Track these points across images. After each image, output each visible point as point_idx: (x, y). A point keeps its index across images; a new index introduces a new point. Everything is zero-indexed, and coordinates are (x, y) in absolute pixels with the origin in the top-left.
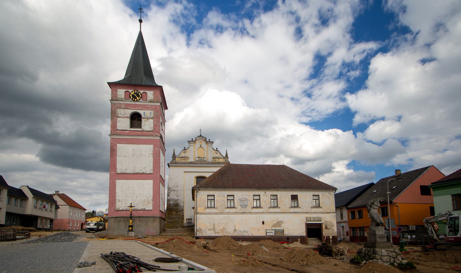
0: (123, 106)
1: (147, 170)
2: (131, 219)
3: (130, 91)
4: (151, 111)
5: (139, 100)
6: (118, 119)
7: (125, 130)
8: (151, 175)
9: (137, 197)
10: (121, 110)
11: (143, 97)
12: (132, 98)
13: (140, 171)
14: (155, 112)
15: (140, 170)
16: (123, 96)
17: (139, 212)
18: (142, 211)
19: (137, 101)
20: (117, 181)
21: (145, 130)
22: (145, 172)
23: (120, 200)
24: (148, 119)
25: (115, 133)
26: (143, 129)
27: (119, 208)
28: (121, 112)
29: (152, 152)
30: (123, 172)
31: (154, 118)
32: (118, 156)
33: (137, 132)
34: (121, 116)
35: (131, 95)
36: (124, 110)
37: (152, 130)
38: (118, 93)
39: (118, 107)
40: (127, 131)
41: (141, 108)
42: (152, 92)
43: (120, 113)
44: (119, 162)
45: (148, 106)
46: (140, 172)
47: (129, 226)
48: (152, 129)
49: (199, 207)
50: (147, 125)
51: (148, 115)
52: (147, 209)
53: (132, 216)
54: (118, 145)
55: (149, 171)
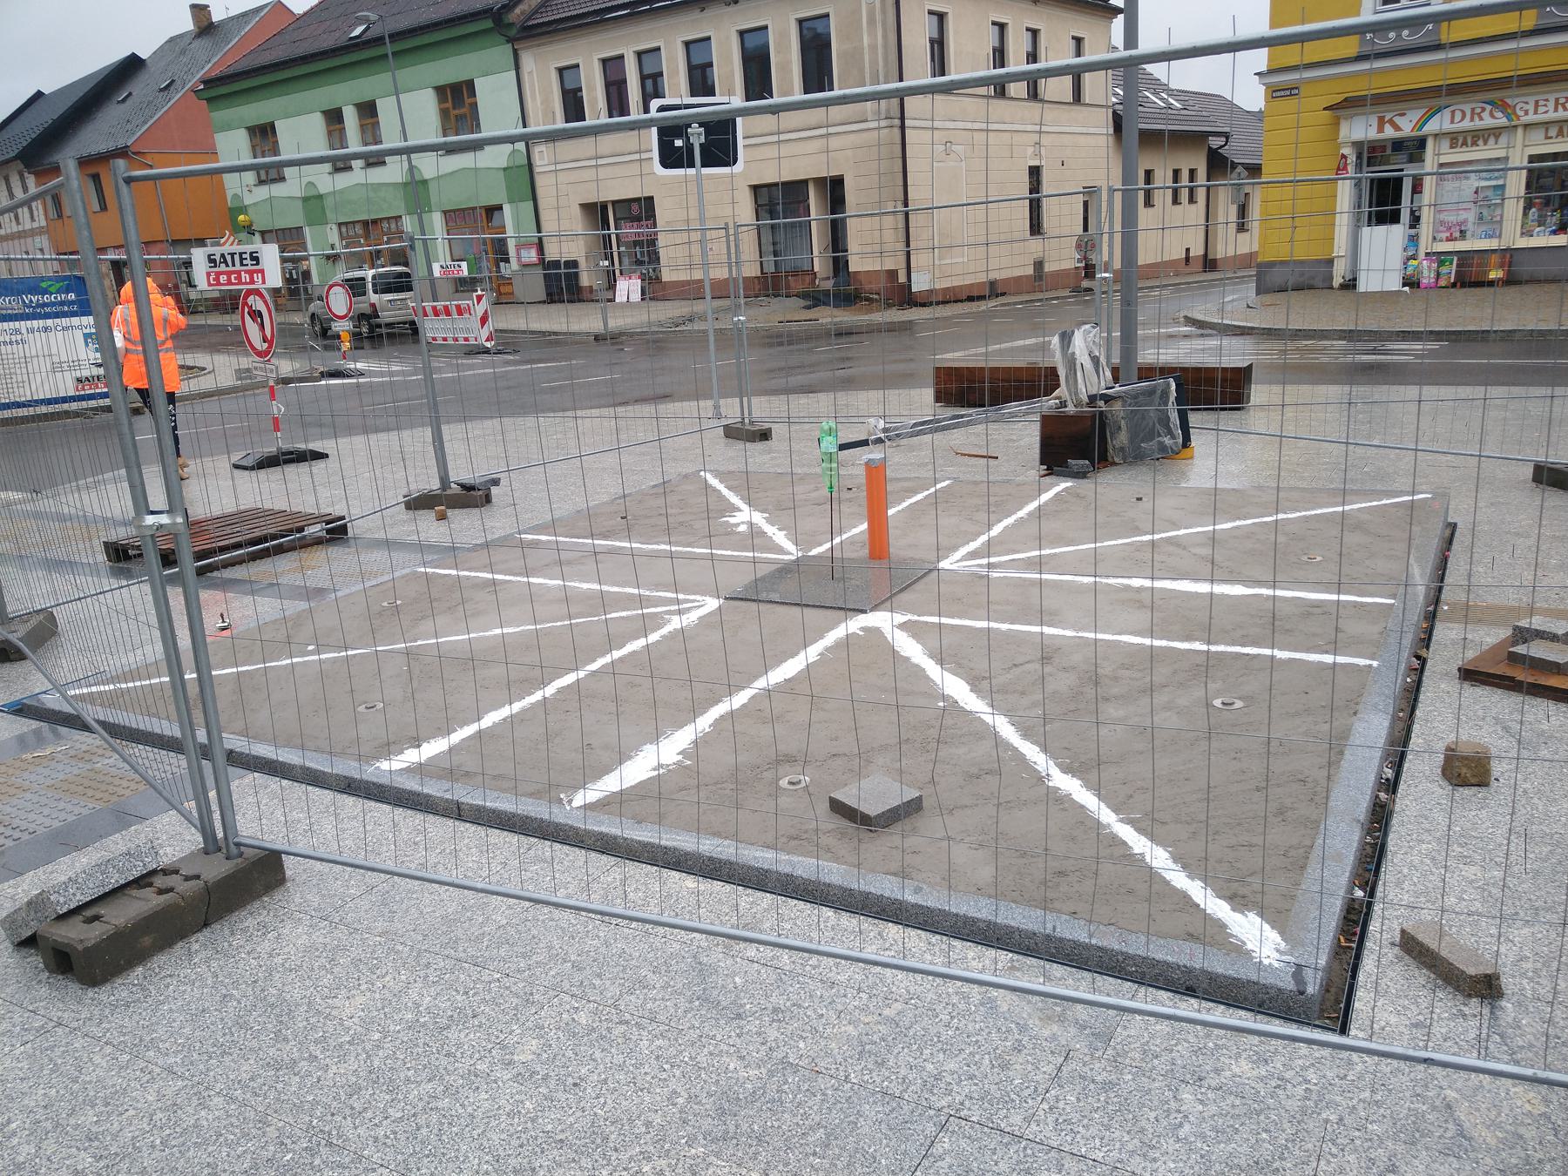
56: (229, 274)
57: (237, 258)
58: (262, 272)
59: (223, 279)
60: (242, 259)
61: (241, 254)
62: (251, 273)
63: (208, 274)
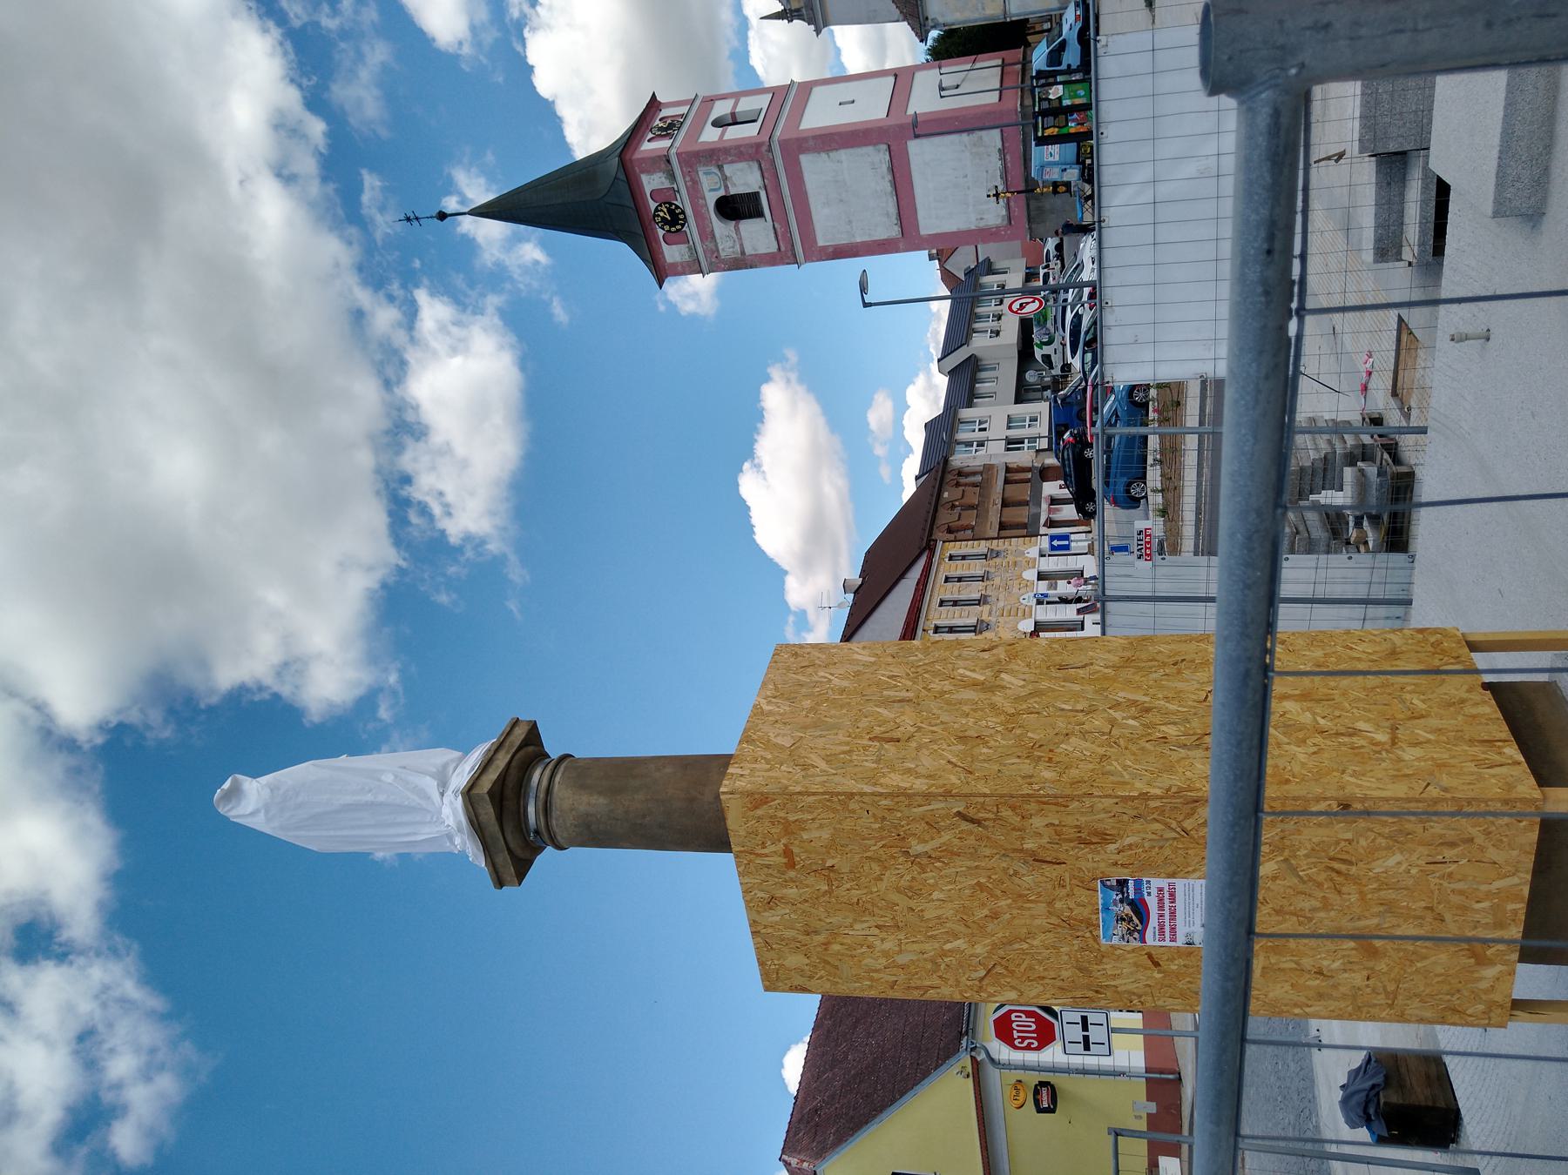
0: (711, 245)
1: (881, 161)
2: (1033, 191)
3: (661, 233)
4: (700, 173)
5: (677, 207)
6: (749, 251)
7: (776, 233)
8: (891, 148)
9: (966, 176)
10: (720, 248)
11: (667, 199)
12: (679, 227)
13: (887, 179)
14: (700, 162)
15: (883, 178)
16: (683, 247)
17: (1009, 165)
18: (1008, 157)
19: (683, 212)
20: (923, 232)
21: (761, 184)
22: (885, 167)
23: (979, 217)
24: (725, 178)
25: (790, 253)
26: (760, 187)
27: (1003, 216)
28: (727, 249)
29: (824, 155)
30: (896, 222)
31: (720, 163)
32: (853, 240)
33: (773, 202)
34: (738, 247)
35: (673, 229)
36: (718, 241)
37: (755, 165)
38: (678, 259)
39: (715, 255)
40: (776, 226)
41: (700, 201)
42: (644, 178)
43: (731, 250)
44: (870, 235)
45: (688, 184)
46: (890, 177)
47: (1055, 192)
48: (751, 163)
49: (983, 9)
50: (745, 179)
51: (716, 179)
52: (1001, 143)
53: (1022, 187)
54: (821, 243)
55: (881, 155)
56: (1146, 548)
57: (1140, 542)
58: (1146, 529)
59: (1148, 552)
60: (1140, 540)
61: (1138, 540)
62: (1146, 536)
63: (1146, 560)
